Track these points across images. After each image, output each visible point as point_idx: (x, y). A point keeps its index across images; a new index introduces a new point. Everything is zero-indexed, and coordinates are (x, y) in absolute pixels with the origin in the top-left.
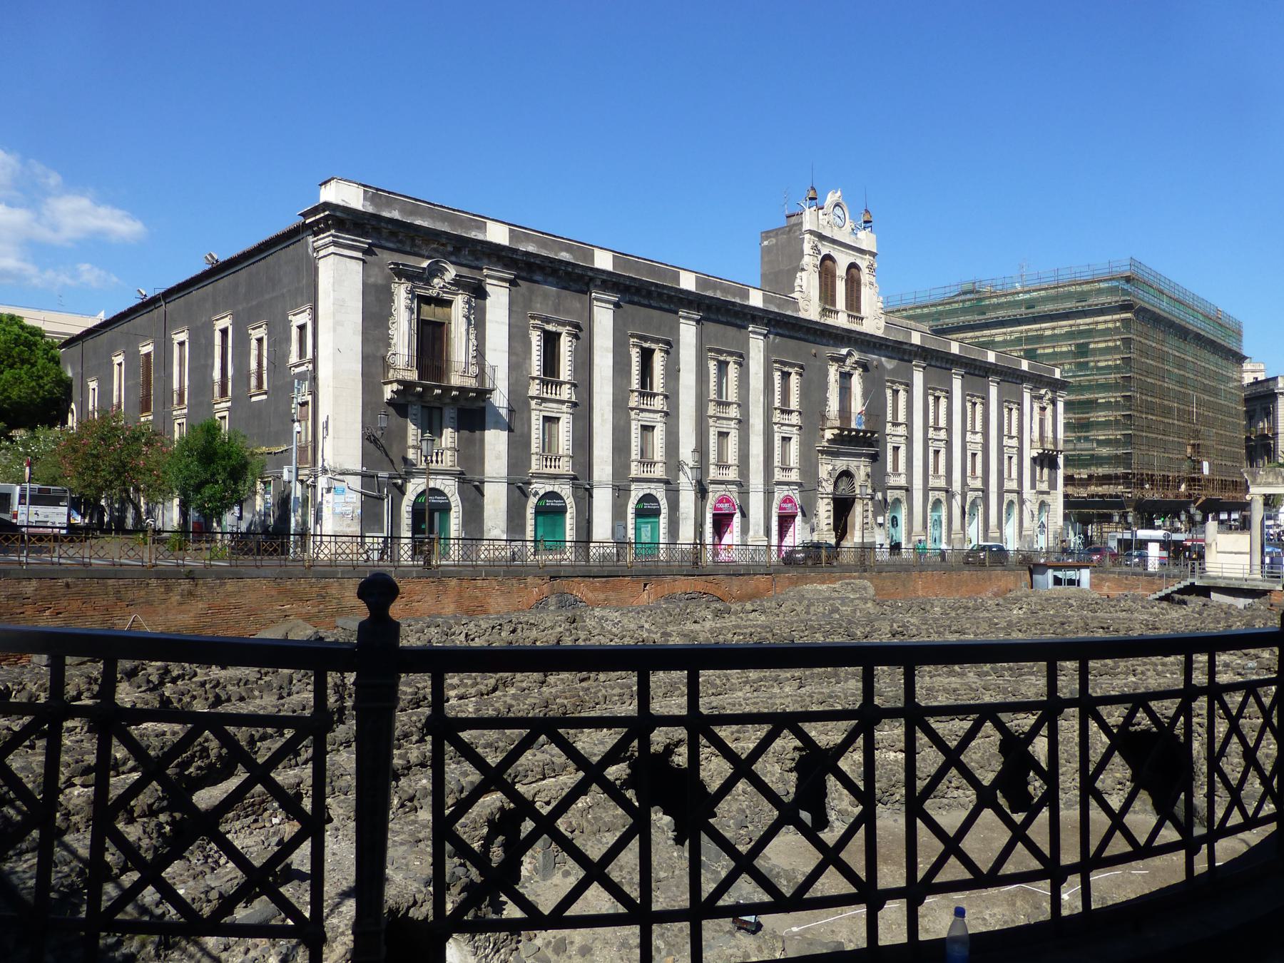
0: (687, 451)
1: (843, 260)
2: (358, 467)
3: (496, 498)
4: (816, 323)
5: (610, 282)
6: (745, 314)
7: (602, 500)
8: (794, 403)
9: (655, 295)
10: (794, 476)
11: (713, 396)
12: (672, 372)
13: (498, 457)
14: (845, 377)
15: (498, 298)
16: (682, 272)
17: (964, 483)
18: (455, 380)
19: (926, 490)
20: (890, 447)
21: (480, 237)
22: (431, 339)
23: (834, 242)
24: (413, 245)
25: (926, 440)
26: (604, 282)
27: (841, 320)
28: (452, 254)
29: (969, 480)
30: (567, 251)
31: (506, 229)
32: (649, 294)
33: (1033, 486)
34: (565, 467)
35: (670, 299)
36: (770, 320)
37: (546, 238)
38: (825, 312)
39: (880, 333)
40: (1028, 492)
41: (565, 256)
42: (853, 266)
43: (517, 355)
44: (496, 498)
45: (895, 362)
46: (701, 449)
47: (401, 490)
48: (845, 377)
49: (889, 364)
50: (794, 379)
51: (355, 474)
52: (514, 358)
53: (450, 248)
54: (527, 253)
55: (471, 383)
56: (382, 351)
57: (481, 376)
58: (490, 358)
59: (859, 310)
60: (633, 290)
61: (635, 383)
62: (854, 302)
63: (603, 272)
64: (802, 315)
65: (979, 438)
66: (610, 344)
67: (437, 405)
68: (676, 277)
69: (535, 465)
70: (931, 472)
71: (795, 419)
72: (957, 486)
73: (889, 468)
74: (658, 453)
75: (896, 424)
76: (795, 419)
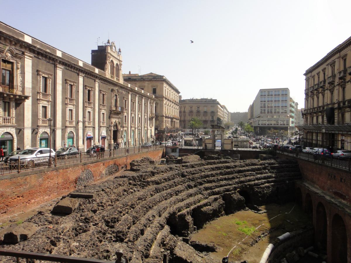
15: (28, 62)
16: (79, 61)
19: (131, 127)
21: (23, 40)
23: (113, 56)
25: (131, 114)
26: (60, 61)
27: (115, 80)
30: (49, 49)
31: (31, 38)
32: (72, 67)
33: (150, 126)
35: (77, 69)
36: (100, 78)
37: (42, 43)
38: (112, 77)
39: (122, 84)
40: (149, 127)
41: (48, 51)
45: (126, 92)
49: (124, 93)
53: (13, 43)
60: (68, 65)
68: (78, 62)
70: (132, 123)
71: (106, 108)
72: (136, 126)
76: (106, 108)
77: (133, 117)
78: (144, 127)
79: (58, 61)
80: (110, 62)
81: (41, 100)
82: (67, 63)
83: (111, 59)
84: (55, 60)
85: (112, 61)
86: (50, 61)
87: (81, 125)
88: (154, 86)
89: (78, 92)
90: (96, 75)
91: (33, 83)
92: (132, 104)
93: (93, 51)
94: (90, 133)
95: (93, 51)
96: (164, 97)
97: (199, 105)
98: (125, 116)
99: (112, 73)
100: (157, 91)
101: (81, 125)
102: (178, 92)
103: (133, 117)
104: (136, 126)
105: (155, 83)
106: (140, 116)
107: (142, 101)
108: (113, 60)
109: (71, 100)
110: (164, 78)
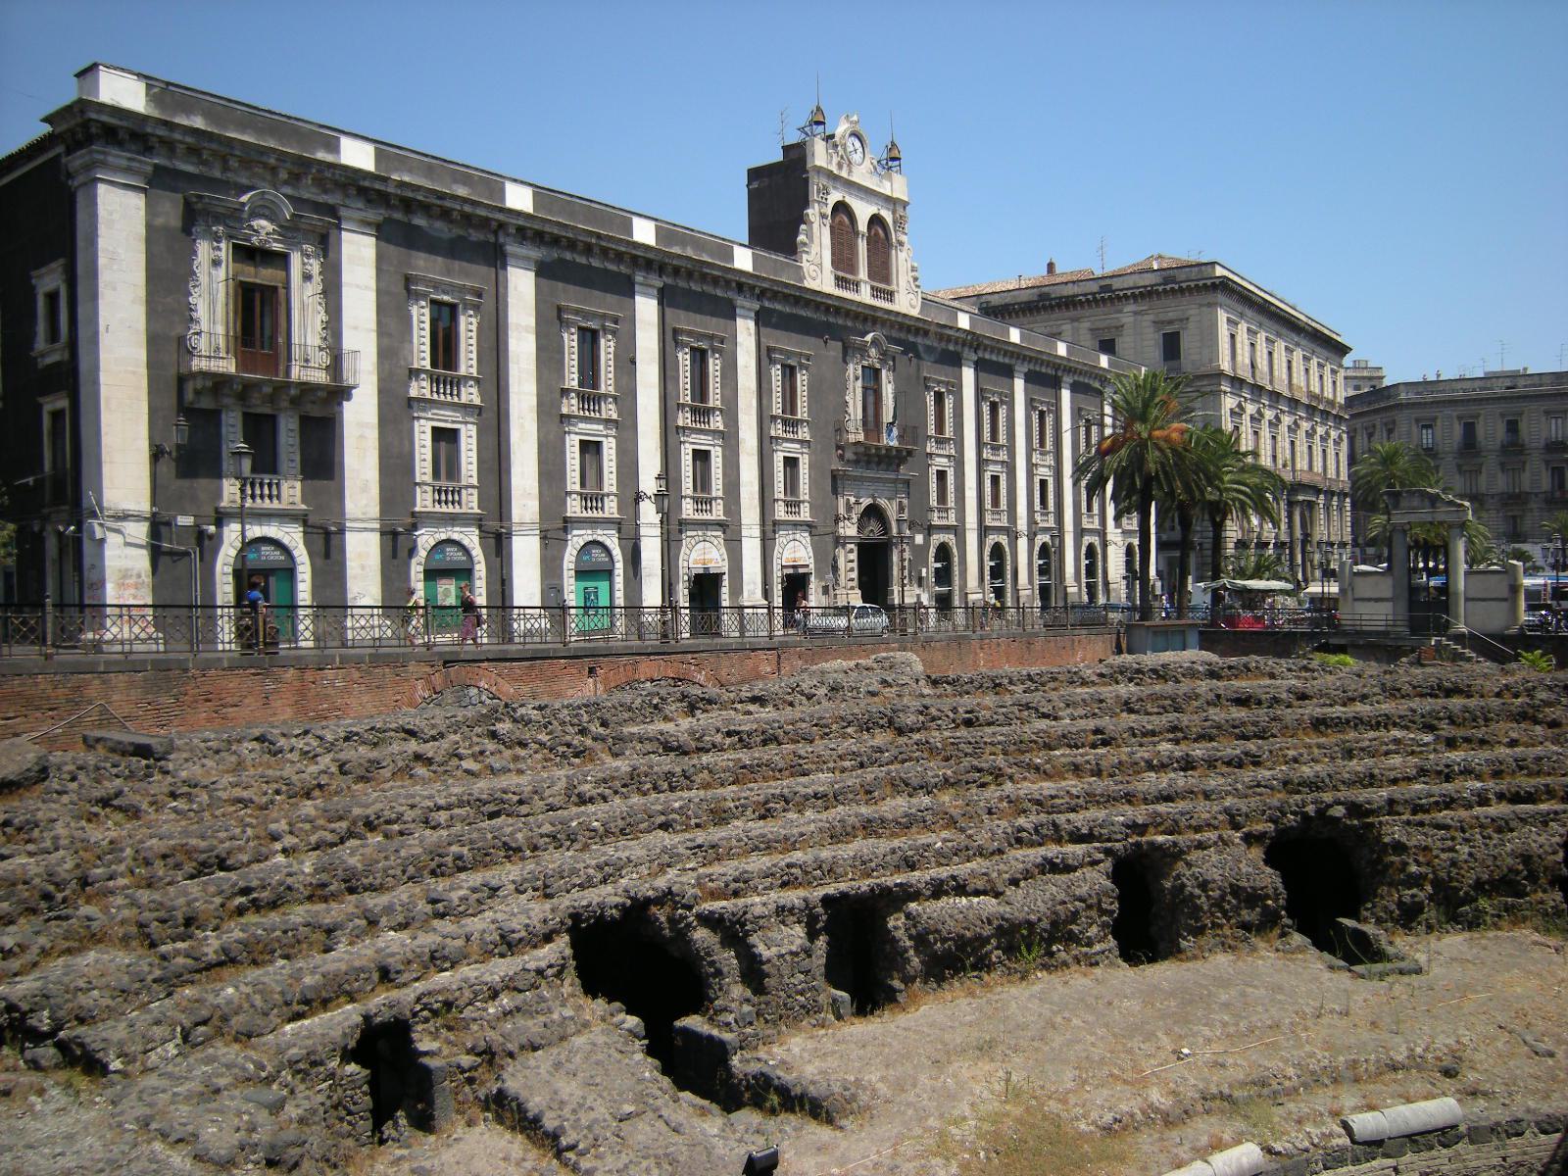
0: (648, 483)
1: (863, 211)
2: (144, 506)
3: (363, 552)
4: (829, 296)
5: (529, 231)
6: (728, 282)
7: (526, 551)
8: (802, 412)
9: (596, 250)
10: (805, 514)
11: (686, 398)
12: (627, 363)
13: (365, 489)
14: (872, 375)
15: (359, 252)
16: (636, 221)
17: (1032, 521)
18: (297, 373)
20: (933, 470)
21: (329, 158)
22: (258, 313)
24: (226, 169)
25: (981, 464)
27: (865, 296)
28: (286, 183)
29: (1038, 517)
30: (465, 184)
34: (471, 503)
37: (436, 165)
38: (840, 282)
39: (915, 312)
41: (462, 191)
42: (876, 220)
43: (390, 335)
44: (363, 552)
46: (668, 473)
47: (217, 540)
48: (872, 375)
50: (802, 379)
51: (137, 517)
52: (386, 341)
53: (283, 175)
54: (402, 184)
55: (320, 377)
56: (179, 330)
57: (336, 365)
58: (349, 342)
59: (887, 279)
61: (572, 380)
62: (881, 271)
63: (519, 214)
64: (809, 284)
65: (1050, 460)
66: (532, 321)
67: (267, 410)
68: (628, 228)
69: (424, 501)
70: (988, 506)
72: (1022, 524)
73: (933, 502)
74: (610, 482)
75: (940, 442)
76: (804, 433)
77: (1043, 483)
78: (1080, 532)
79: (512, 231)
80: (828, 211)
81: (575, 417)
82: (556, 232)
83: (835, 196)
84: (494, 224)
85: (841, 207)
86: (471, 231)
87: (649, 513)
88: (1170, 322)
89: (633, 362)
90: (729, 276)
91: (382, 331)
92: (986, 409)
93: (754, 174)
94: (703, 553)
95: (754, 174)
96: (1220, 375)
97: (1473, 408)
98: (942, 475)
99: (843, 260)
100: (1187, 343)
101: (649, 513)
102: (1342, 350)
103: (1043, 483)
104: (1022, 524)
105: (1171, 309)
106: (1044, 472)
107: (1058, 399)
108: (849, 200)
109: (701, 412)
110: (1219, 271)
